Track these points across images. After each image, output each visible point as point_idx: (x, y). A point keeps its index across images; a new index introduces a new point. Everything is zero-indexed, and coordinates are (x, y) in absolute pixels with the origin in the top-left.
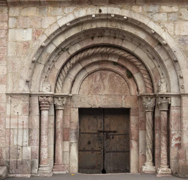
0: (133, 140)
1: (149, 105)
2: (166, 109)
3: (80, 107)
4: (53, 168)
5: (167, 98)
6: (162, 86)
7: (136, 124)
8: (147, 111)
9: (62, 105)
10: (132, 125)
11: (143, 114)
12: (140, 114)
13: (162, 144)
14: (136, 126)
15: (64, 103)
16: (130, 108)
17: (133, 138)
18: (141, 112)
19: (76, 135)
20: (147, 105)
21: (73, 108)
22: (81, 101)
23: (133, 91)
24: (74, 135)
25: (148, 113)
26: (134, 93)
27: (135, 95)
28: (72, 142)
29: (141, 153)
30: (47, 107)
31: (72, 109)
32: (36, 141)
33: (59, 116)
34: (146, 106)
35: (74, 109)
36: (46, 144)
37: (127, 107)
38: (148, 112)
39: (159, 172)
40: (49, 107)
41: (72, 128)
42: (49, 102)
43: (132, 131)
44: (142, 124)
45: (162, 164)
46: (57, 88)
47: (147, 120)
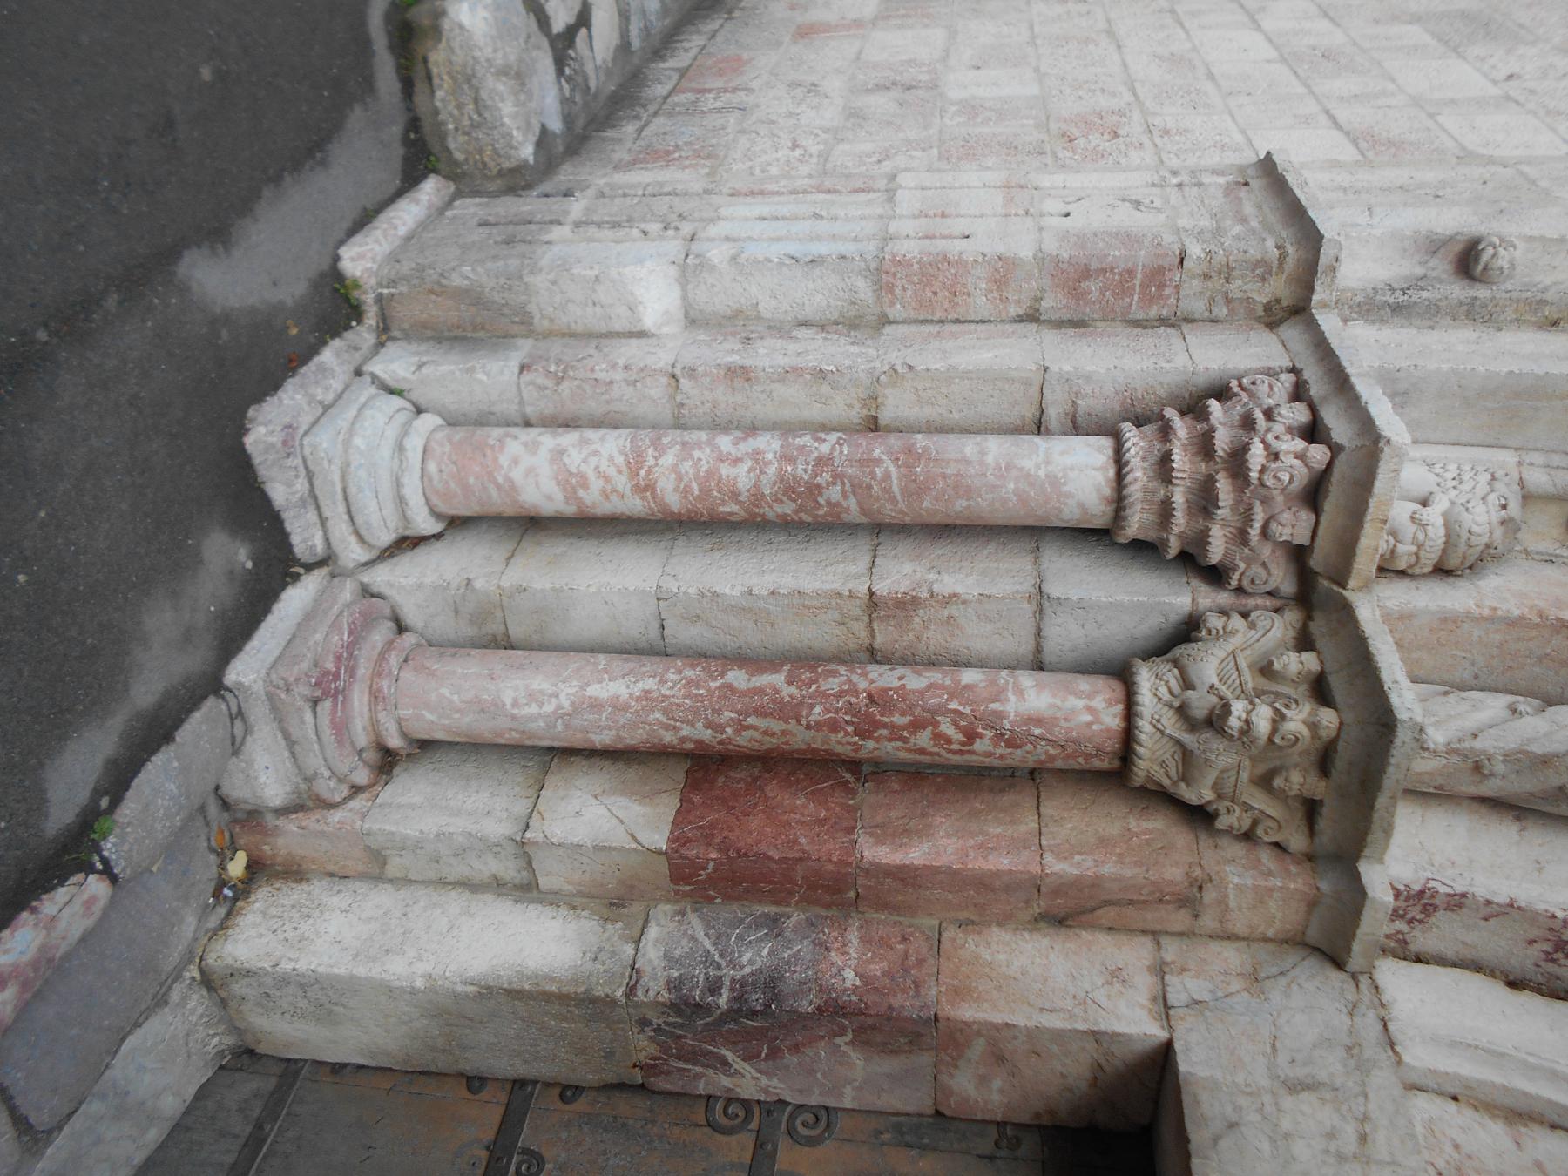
3: (1190, 1063)
4: (367, 592)
9: (1201, 702)
15: (1238, 708)
19: (742, 988)
21: (1160, 970)
22: (1296, 1087)
24: (754, 956)
28: (653, 932)
30: (1166, 459)
31: (1134, 955)
32: (735, 358)
33: (1040, 686)
35: (1144, 984)
36: (669, 459)
40: (1165, 511)
41: (853, 936)
42: (1237, 461)
46: (1446, 693)
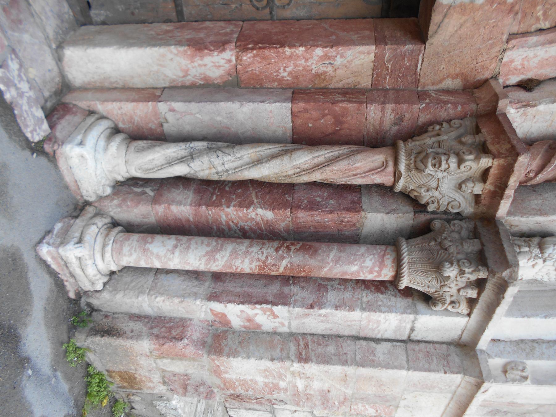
0: (237, 58)
1: (434, 184)
2: (404, 283)
5: (472, 302)
6: (537, 268)
7: (325, 73)
8: (402, 167)
10: (319, 52)
11: (381, 122)
12: (383, 110)
13: (218, 256)
14: (318, 75)
16: (424, 43)
17: (247, 57)
18: (393, 110)
20: (440, 175)
23: (530, 53)
25: (384, 165)
26: (517, 63)
27: (503, 70)
29: (172, 110)
34: (430, 169)
37: (436, 18)
38: (391, 168)
39: (70, 246)
43: (288, 51)
44: (324, 116)
45: (120, 252)
47: (343, 165)
